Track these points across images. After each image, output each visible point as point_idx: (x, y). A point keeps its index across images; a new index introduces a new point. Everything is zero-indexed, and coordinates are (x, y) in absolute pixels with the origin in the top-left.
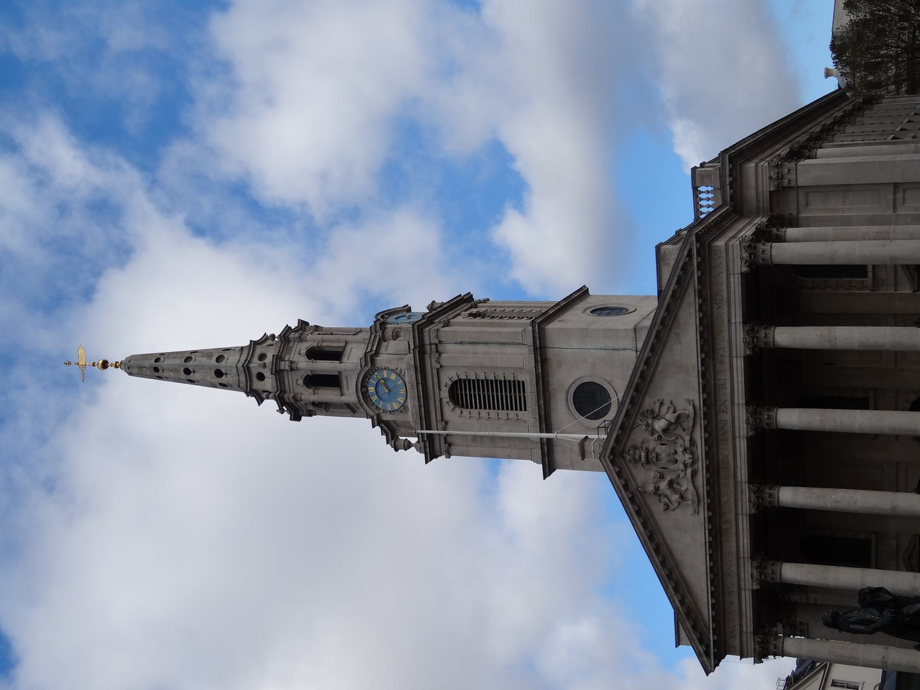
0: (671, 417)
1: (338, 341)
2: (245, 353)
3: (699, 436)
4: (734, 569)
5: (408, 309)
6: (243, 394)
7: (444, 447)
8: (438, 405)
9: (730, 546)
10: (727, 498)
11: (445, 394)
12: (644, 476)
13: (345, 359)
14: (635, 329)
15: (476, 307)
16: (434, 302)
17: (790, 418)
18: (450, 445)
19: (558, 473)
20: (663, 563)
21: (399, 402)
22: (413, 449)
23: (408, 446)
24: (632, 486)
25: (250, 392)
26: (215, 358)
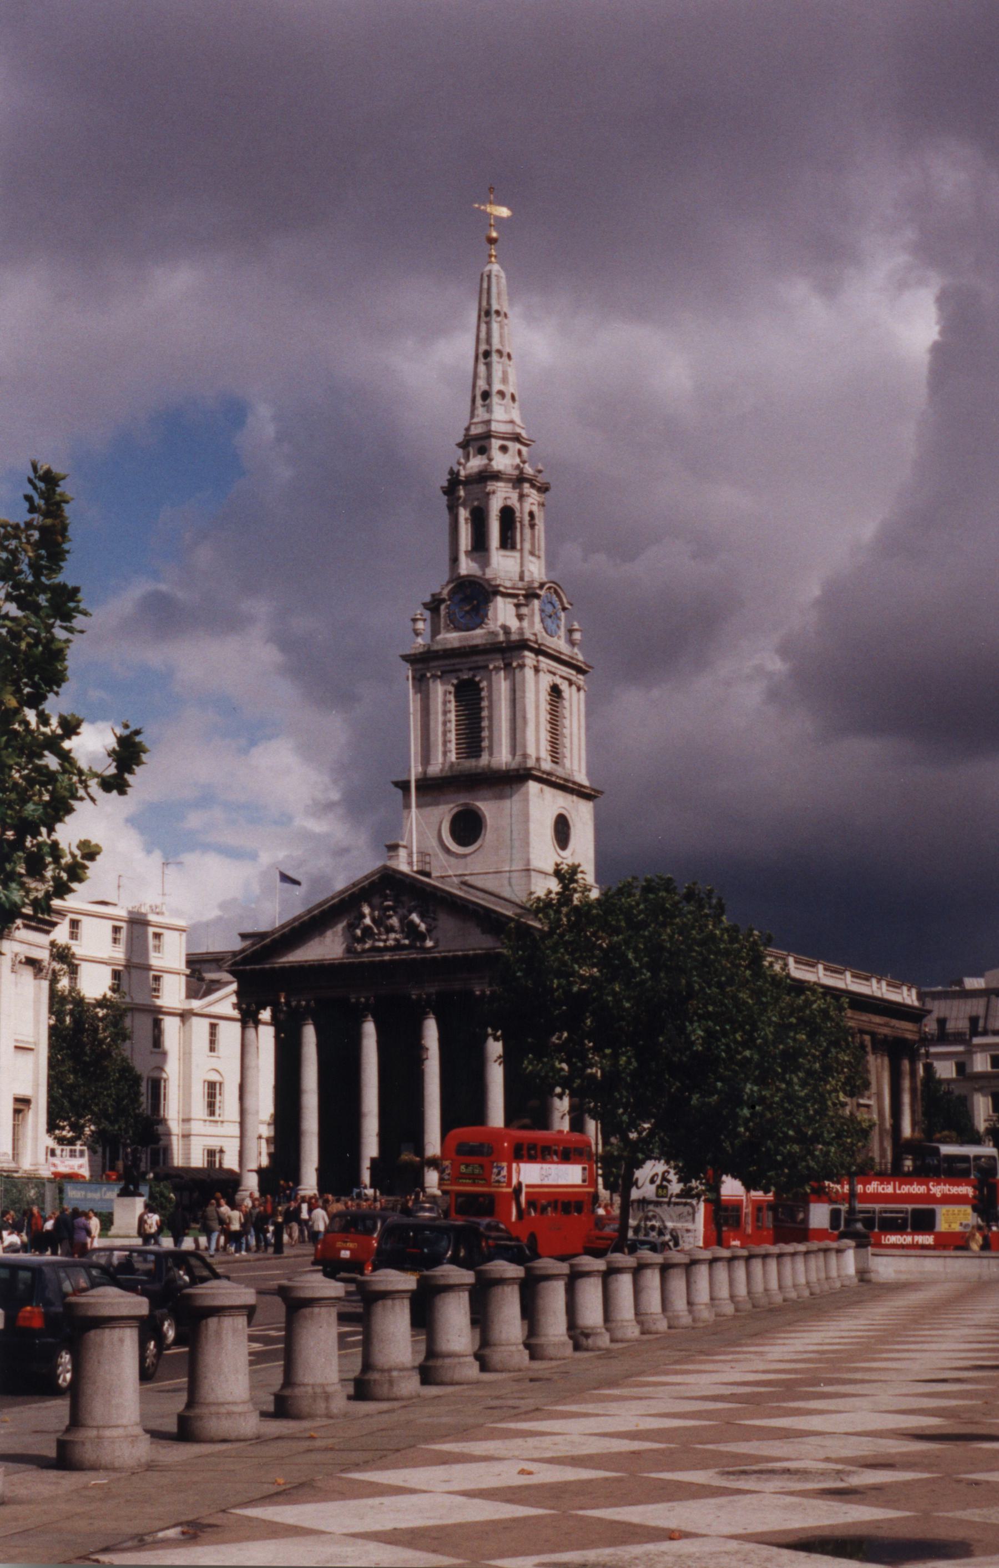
8: (457, 667)
13: (502, 552)
14: (528, 870)
15: (571, 683)
26: (502, 387)
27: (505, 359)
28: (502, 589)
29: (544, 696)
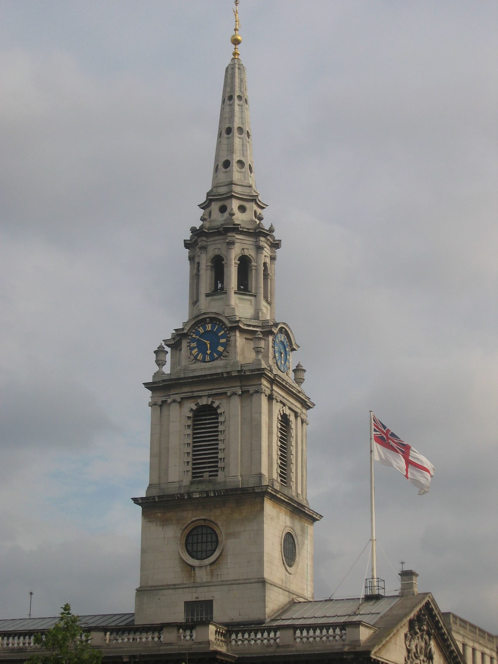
1: (257, 288)
2: (247, 191)
6: (209, 188)
7: (159, 401)
8: (195, 394)
11: (204, 401)
15: (296, 415)
16: (304, 371)
18: (161, 406)
19: (140, 508)
21: (198, 355)
22: (156, 368)
23: (160, 363)
25: (211, 199)
27: (245, 135)
28: (241, 326)
29: (276, 425)
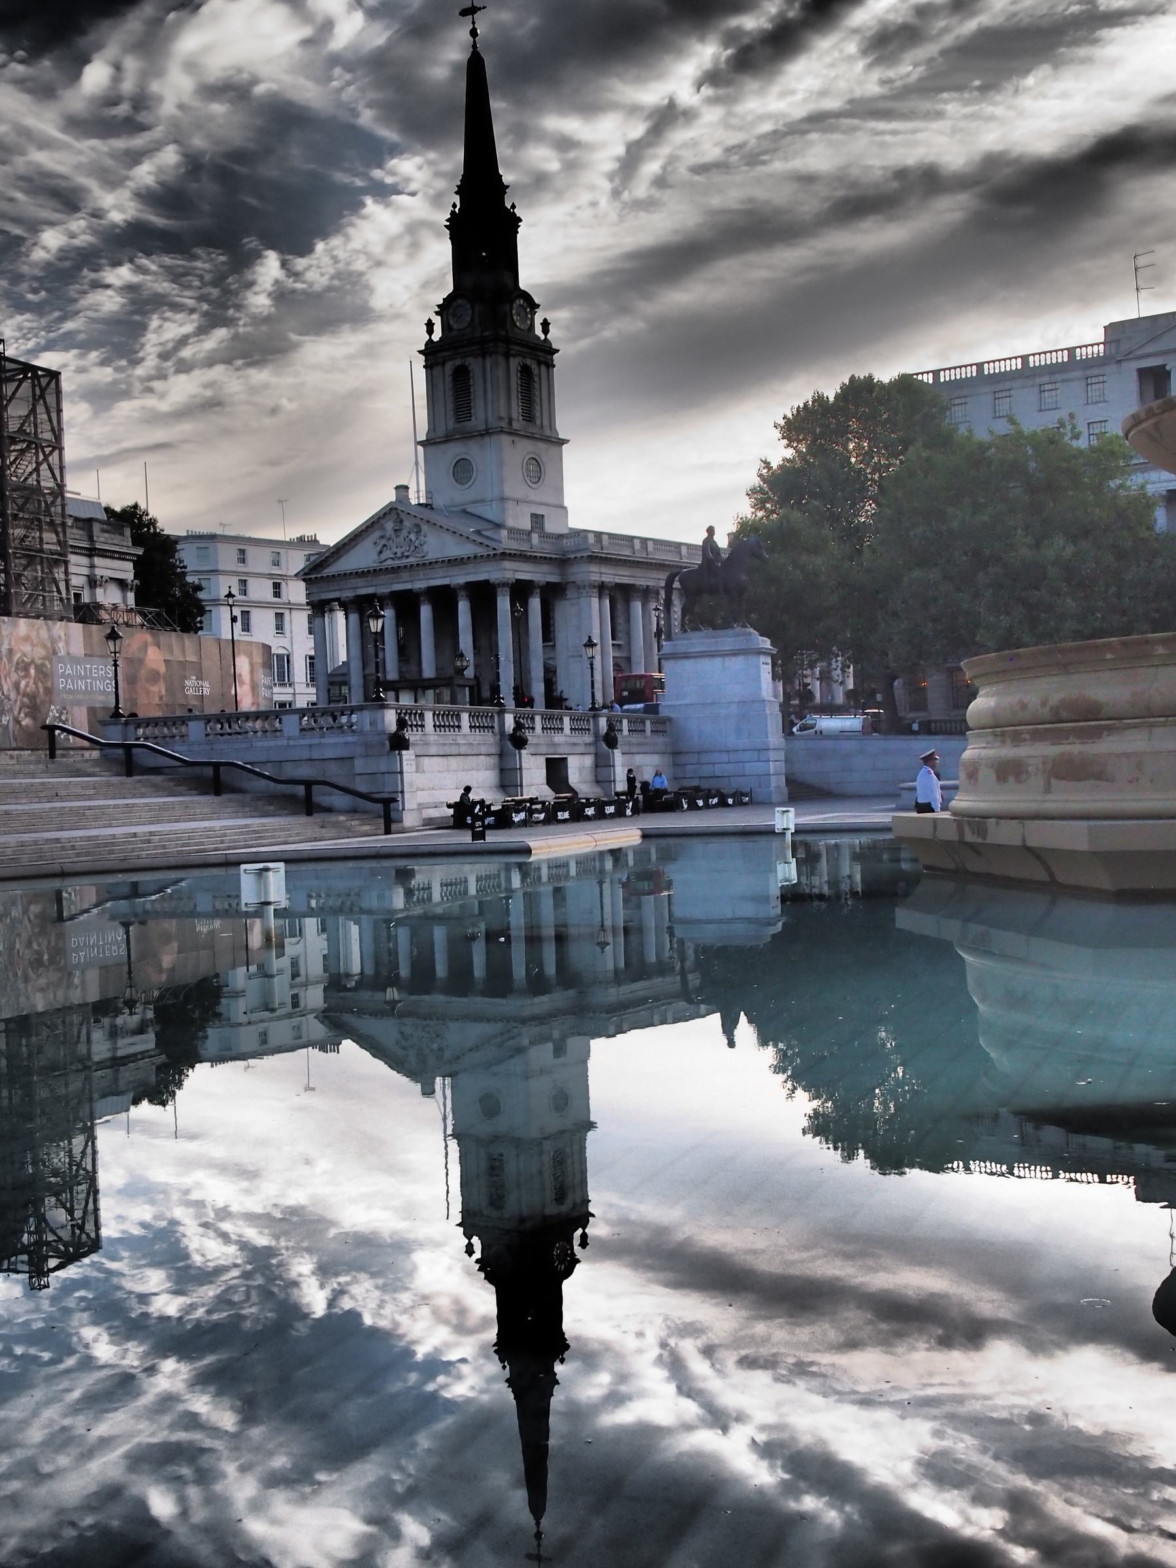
0: (417, 544)
3: (411, 560)
4: (350, 586)
5: (534, 306)
9: (360, 582)
10: (384, 578)
11: (458, 362)
12: (389, 525)
15: (539, 363)
17: (426, 612)
20: (344, 545)
22: (428, 337)
24: (382, 521)
